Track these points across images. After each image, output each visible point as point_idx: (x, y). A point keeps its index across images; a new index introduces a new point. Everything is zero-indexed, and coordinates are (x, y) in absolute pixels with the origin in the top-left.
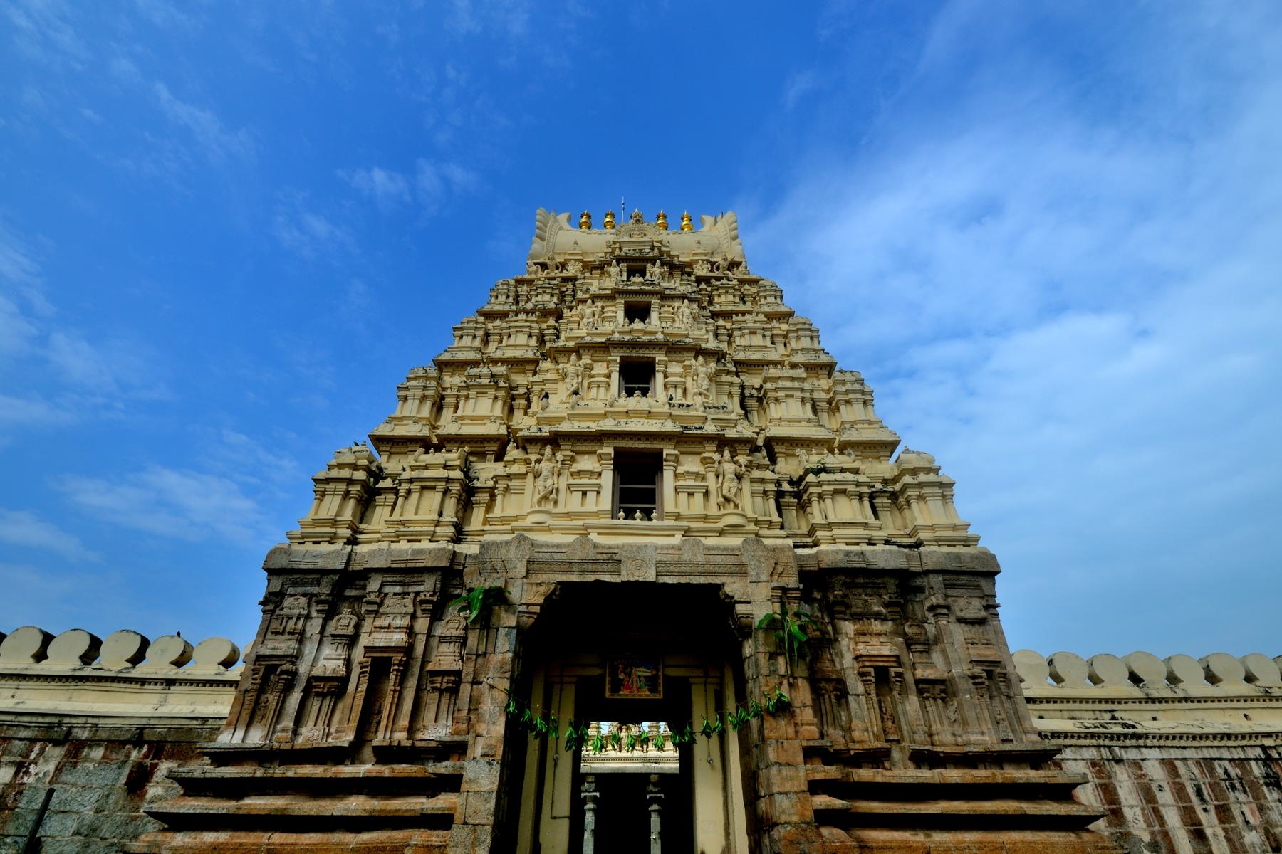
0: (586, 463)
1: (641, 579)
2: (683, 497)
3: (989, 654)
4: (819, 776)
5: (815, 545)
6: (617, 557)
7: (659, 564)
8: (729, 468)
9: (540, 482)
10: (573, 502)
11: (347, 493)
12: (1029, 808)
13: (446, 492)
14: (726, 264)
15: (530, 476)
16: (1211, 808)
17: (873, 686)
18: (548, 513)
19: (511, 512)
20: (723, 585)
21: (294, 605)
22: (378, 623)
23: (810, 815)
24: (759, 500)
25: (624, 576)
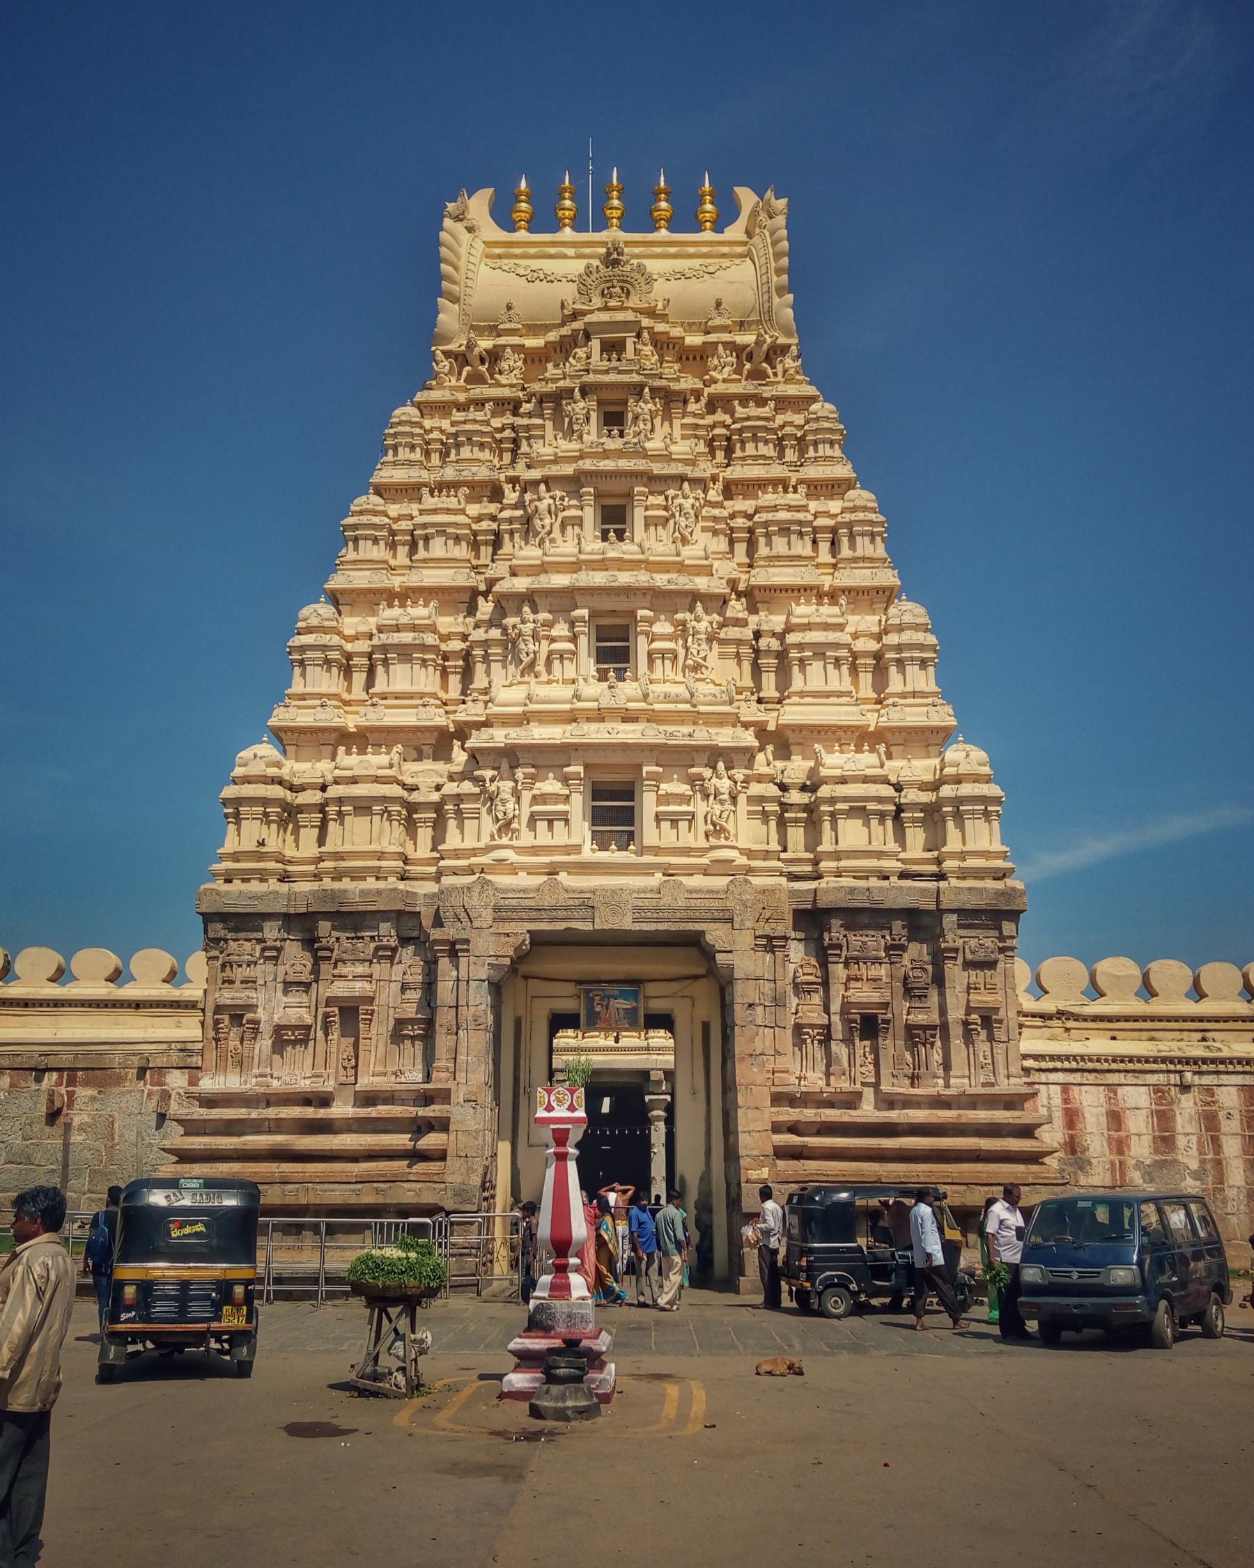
0: (550, 785)
1: (615, 927)
2: (666, 825)
4: (782, 1118)
6: (590, 903)
7: (637, 909)
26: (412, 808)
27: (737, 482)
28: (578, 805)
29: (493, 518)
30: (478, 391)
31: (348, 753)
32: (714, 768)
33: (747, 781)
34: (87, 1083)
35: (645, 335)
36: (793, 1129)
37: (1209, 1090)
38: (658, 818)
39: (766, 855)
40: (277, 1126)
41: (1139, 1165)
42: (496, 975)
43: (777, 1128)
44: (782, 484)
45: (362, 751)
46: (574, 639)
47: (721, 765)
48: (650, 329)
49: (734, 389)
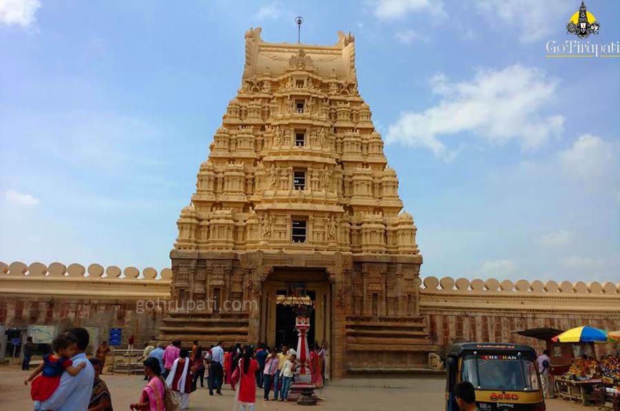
3: (410, 290)
5: (362, 252)
7: (306, 261)
8: (333, 223)
9: (263, 228)
10: (276, 237)
11: (191, 228)
12: (409, 333)
13: (229, 228)
14: (346, 85)
15: (260, 225)
16: (494, 332)
17: (371, 300)
18: (268, 240)
19: (254, 239)
20: (326, 268)
21: (183, 270)
22: (214, 277)
23: (345, 334)
24: (343, 235)
25: (294, 265)
26: (236, 227)
27: (338, 128)
28: (289, 228)
29: (262, 136)
30: (257, 95)
31: (217, 209)
32: (330, 218)
33: (341, 222)
34: (129, 309)
35: (310, 80)
36: (352, 327)
37: (473, 317)
38: (313, 232)
39: (346, 245)
40: (196, 324)
41: (452, 339)
42: (264, 279)
43: (347, 327)
44: (353, 129)
45: (221, 209)
46: (288, 176)
47: (333, 218)
48: (312, 78)
49: (337, 98)
